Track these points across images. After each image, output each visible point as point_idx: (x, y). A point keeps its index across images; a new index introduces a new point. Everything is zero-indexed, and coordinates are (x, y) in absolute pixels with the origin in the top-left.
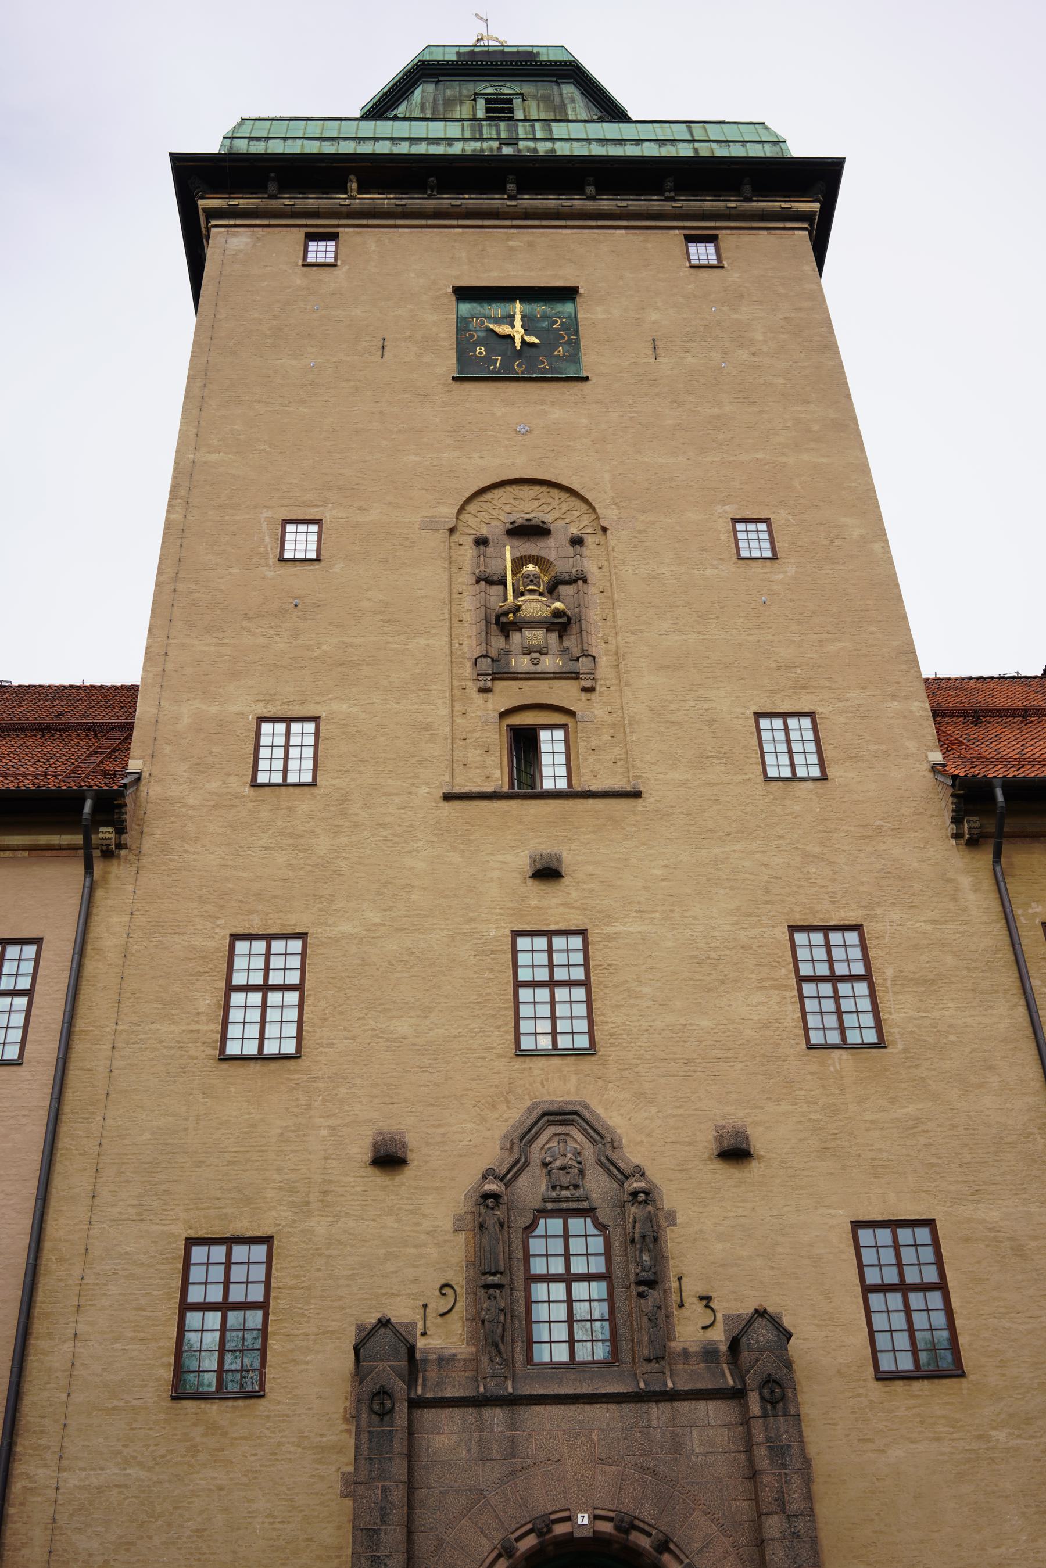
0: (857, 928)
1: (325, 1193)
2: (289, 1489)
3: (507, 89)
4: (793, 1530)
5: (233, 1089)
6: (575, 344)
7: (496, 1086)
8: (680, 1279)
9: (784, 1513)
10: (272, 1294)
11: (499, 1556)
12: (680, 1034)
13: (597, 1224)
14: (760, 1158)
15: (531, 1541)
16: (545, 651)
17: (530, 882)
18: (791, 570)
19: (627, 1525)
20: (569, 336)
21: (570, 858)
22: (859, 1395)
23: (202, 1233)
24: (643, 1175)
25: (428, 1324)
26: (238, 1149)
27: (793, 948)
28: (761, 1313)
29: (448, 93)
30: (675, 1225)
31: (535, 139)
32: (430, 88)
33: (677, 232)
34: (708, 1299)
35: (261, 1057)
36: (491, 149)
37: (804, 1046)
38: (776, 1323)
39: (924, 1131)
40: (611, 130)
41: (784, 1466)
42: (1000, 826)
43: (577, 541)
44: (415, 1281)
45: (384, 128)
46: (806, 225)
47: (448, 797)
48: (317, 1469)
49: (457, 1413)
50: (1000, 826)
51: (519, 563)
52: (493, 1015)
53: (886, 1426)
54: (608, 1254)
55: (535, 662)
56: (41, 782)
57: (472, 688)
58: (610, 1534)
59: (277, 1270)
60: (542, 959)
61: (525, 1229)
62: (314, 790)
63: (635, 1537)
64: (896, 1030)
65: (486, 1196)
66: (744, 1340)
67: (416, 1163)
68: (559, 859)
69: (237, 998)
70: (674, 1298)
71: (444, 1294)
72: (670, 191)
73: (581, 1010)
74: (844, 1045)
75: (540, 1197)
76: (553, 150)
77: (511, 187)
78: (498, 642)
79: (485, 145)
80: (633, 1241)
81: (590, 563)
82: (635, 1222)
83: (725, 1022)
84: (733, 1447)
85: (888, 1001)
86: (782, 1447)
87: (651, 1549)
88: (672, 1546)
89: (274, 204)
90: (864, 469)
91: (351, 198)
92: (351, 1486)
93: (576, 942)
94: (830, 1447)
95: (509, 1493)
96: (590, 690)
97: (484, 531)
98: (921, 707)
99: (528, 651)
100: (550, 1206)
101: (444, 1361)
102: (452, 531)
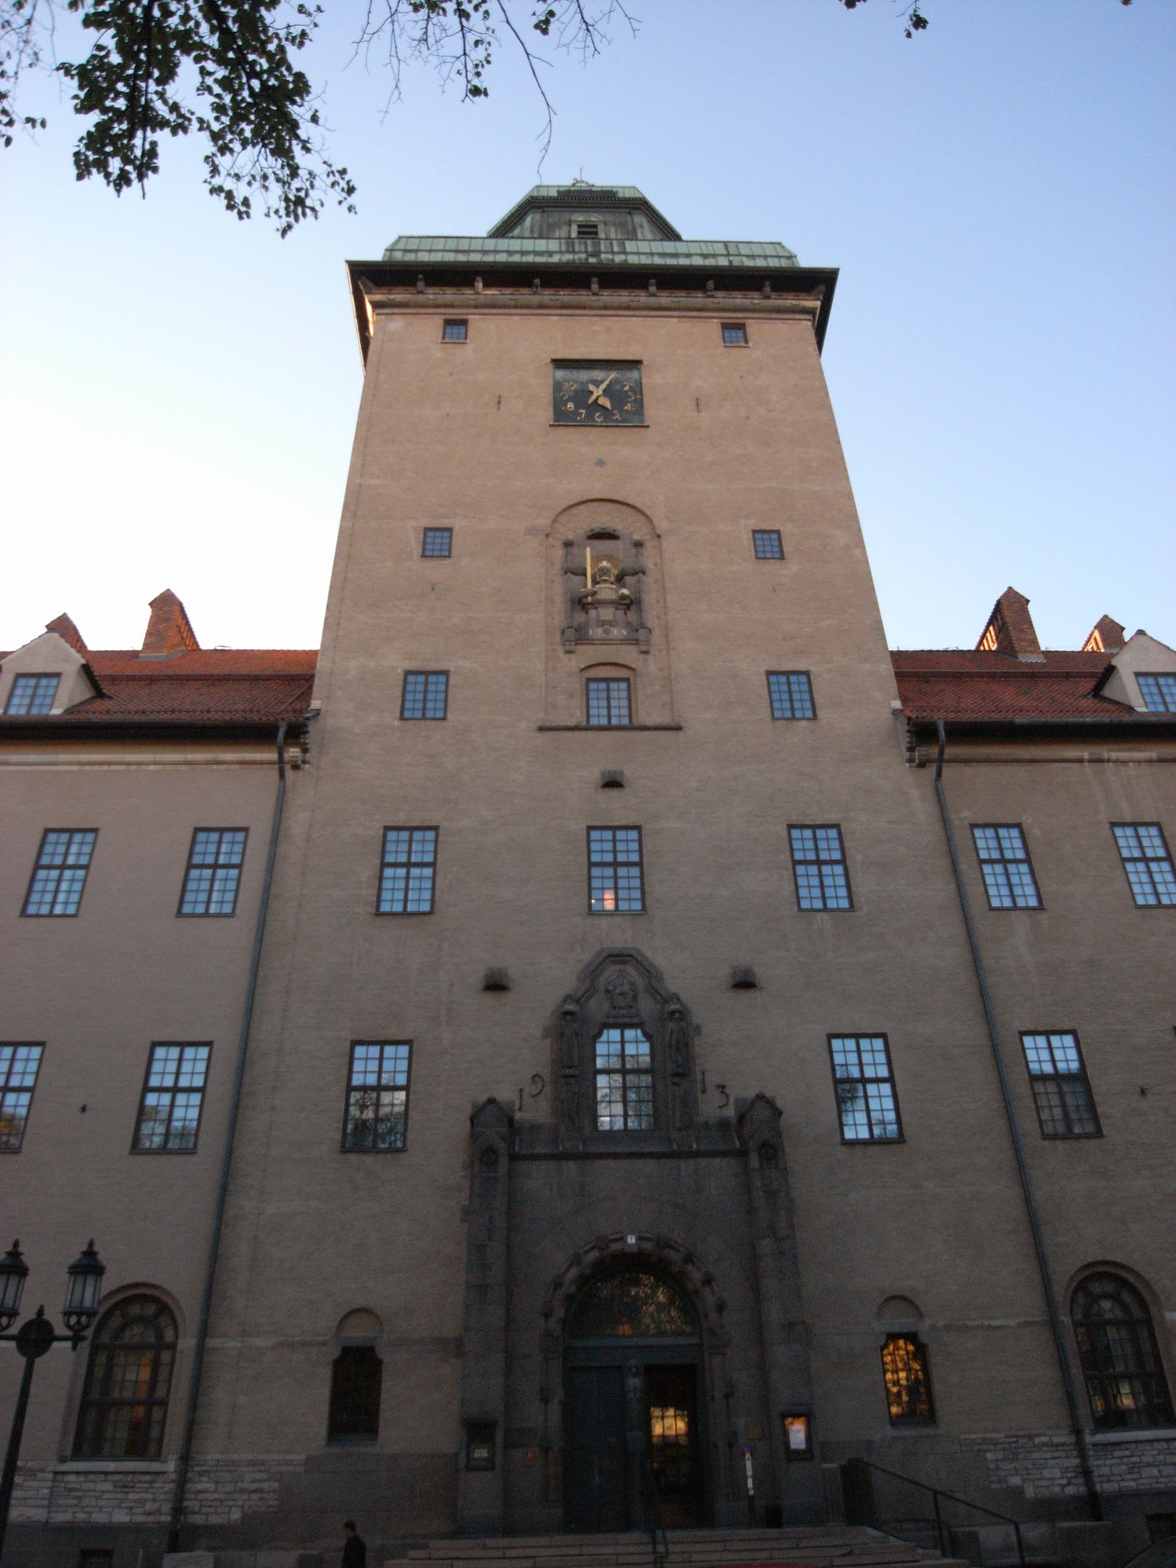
0: (837, 826)
3: (594, 218)
6: (640, 403)
8: (703, 1073)
11: (571, 1265)
13: (645, 1034)
15: (594, 1255)
16: (614, 624)
17: (600, 790)
18: (795, 568)
19: (664, 1243)
20: (635, 394)
21: (628, 772)
23: (362, 1038)
24: (678, 999)
25: (524, 1103)
27: (790, 840)
28: (760, 1097)
29: (550, 220)
30: (700, 1035)
31: (613, 253)
32: (538, 216)
33: (715, 320)
34: (723, 1087)
35: (405, 914)
36: (580, 259)
37: (796, 909)
38: (771, 1104)
40: (669, 246)
42: (941, 753)
43: (638, 545)
45: (503, 244)
46: (810, 317)
47: (541, 729)
50: (941, 753)
51: (596, 559)
55: (606, 632)
56: (248, 715)
57: (560, 650)
60: (609, 846)
62: (444, 723)
63: (669, 1254)
64: (863, 899)
65: (566, 1013)
68: (622, 774)
69: (389, 872)
70: (699, 1086)
72: (711, 291)
73: (636, 883)
74: (825, 909)
76: (626, 260)
77: (595, 287)
78: (580, 617)
79: (576, 257)
80: (670, 1046)
81: (649, 559)
82: (672, 1032)
85: (857, 879)
88: (694, 1259)
89: (421, 298)
90: (849, 495)
91: (477, 293)
92: (467, 1214)
93: (634, 835)
96: (646, 652)
97: (571, 537)
98: (886, 668)
99: (601, 623)
100: (611, 1021)
101: (535, 1128)
102: (547, 535)
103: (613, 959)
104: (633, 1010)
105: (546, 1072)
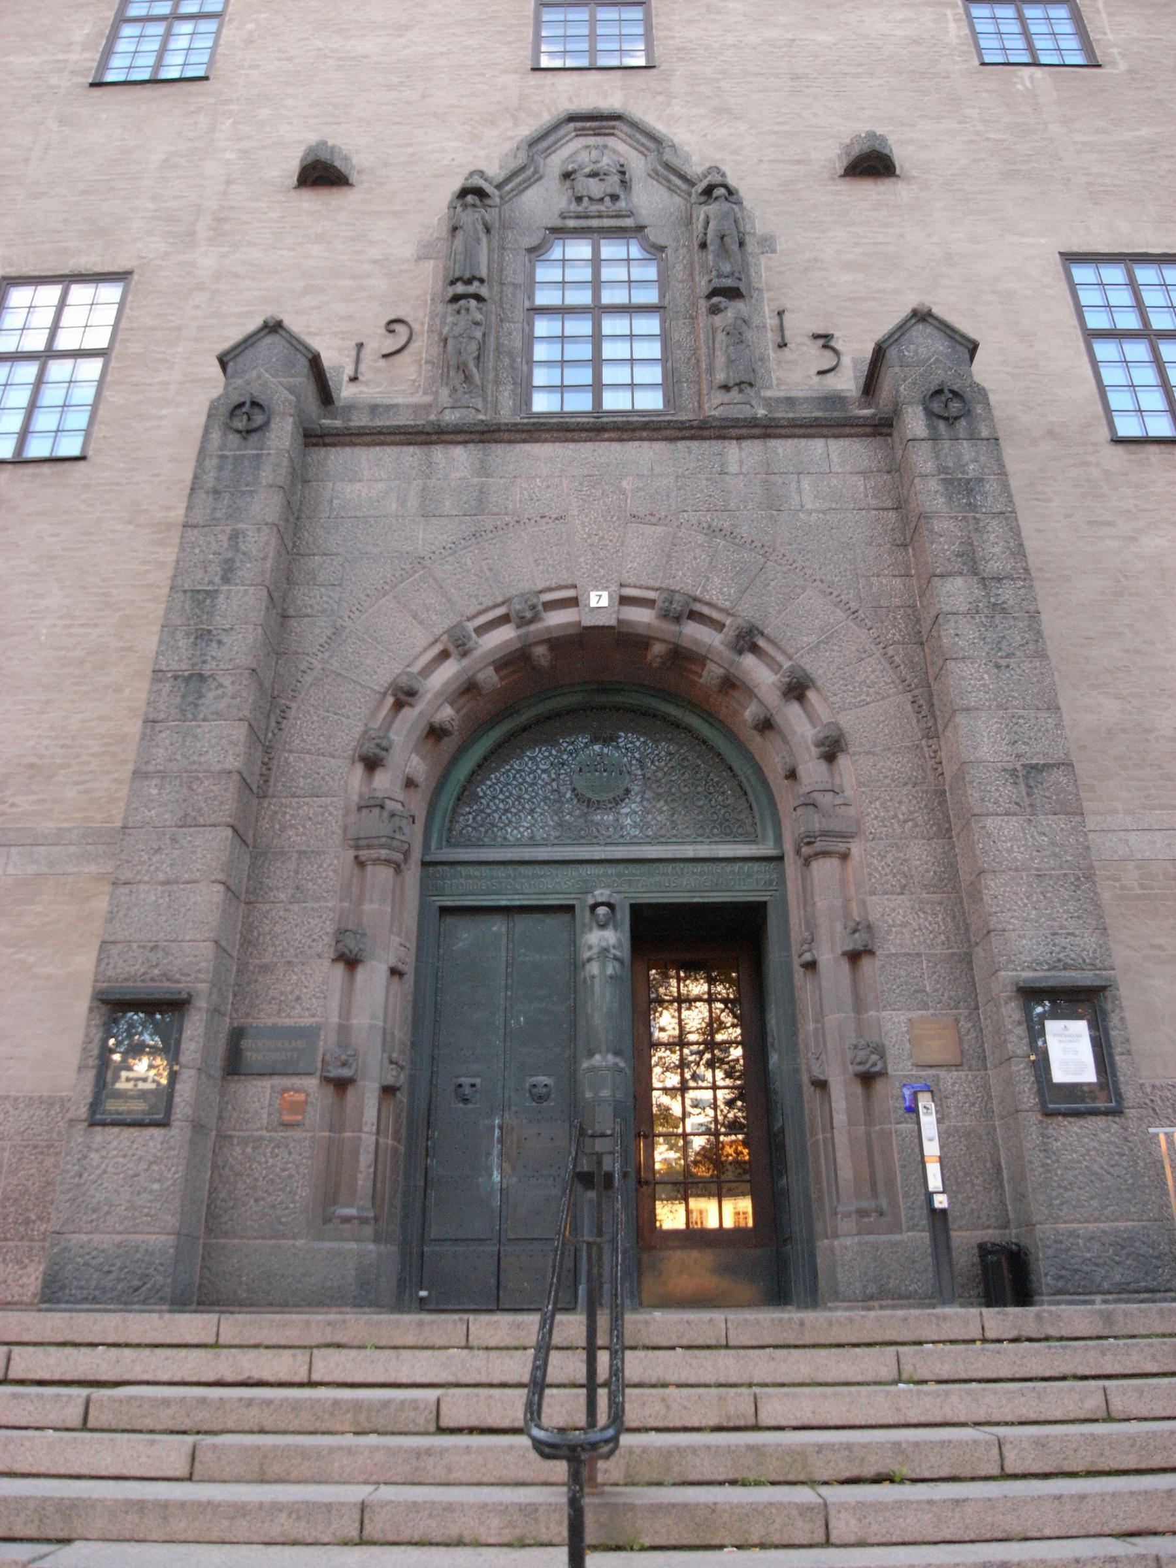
1: (220, 220)
2: (103, 580)
4: (993, 600)
5: (104, 116)
7: (499, 103)
8: (780, 314)
9: (976, 574)
10: (120, 337)
12: (785, 49)
14: (908, 179)
15: (505, 635)
22: (1087, 464)
23: (27, 270)
25: (363, 367)
26: (96, 178)
28: (922, 316)
30: (774, 251)
39: (1167, 156)
41: (972, 507)
44: (348, 318)
48: (155, 553)
49: (388, 455)
52: (501, 32)
53: (1136, 505)
54: (663, 282)
58: (649, 625)
59: (132, 309)
61: (530, 251)
63: (694, 632)
66: (892, 353)
67: (365, 185)
71: (392, 331)
75: (557, 214)
80: (703, 246)
83: (854, 37)
84: (873, 502)
86: (968, 481)
87: (722, 648)
88: (762, 643)
94: (1040, 531)
95: (469, 562)
100: (571, 223)
103: (579, 125)
104: (622, 204)
105: (419, 316)
